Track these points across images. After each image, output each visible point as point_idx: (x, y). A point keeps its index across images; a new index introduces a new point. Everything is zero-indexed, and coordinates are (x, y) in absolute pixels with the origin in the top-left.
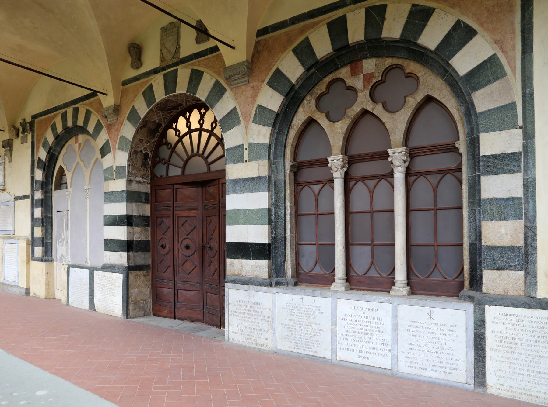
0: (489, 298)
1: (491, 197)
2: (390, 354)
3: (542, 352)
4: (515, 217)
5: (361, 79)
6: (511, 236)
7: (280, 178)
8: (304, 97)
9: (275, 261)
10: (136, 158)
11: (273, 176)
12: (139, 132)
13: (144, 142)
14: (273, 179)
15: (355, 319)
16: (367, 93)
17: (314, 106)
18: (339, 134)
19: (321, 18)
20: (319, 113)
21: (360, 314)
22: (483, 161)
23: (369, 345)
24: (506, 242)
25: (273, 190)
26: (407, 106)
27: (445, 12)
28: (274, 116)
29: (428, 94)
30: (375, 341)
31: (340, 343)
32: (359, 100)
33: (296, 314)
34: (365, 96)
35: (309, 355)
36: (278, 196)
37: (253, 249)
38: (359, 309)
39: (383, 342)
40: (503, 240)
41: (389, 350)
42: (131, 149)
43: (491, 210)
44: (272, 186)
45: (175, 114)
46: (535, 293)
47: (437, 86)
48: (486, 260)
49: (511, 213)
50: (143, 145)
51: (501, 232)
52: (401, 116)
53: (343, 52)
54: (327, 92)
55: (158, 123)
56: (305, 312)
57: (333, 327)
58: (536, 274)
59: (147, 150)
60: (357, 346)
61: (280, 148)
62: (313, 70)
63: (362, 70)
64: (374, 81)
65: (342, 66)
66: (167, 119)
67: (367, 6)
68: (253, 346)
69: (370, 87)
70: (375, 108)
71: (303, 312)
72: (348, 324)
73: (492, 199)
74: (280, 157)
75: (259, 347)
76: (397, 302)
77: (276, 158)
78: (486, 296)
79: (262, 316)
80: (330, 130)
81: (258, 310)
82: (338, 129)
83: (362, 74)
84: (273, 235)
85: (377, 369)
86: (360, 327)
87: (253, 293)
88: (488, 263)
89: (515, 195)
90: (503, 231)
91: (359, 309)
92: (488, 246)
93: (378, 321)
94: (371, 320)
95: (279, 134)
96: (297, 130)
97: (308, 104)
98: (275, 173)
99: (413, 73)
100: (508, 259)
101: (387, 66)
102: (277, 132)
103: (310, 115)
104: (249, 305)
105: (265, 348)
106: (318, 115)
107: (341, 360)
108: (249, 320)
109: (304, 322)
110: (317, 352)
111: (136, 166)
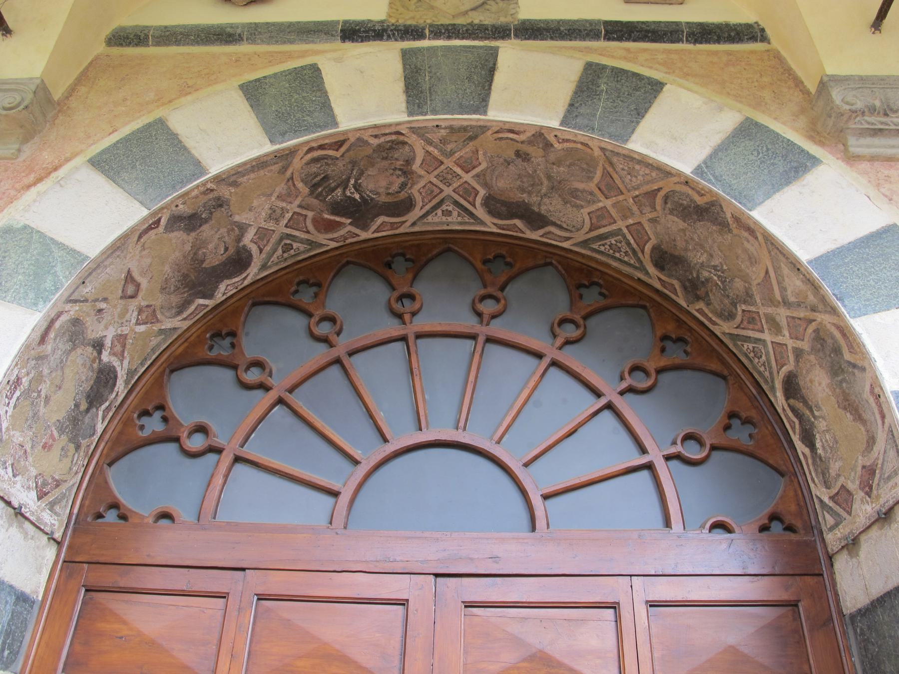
10: (62, 365)
12: (152, 233)
13: (133, 304)
42: (69, 301)
45: (333, 245)
50: (122, 315)
55: (244, 246)
59: (122, 357)
66: (287, 248)
111: (42, 410)
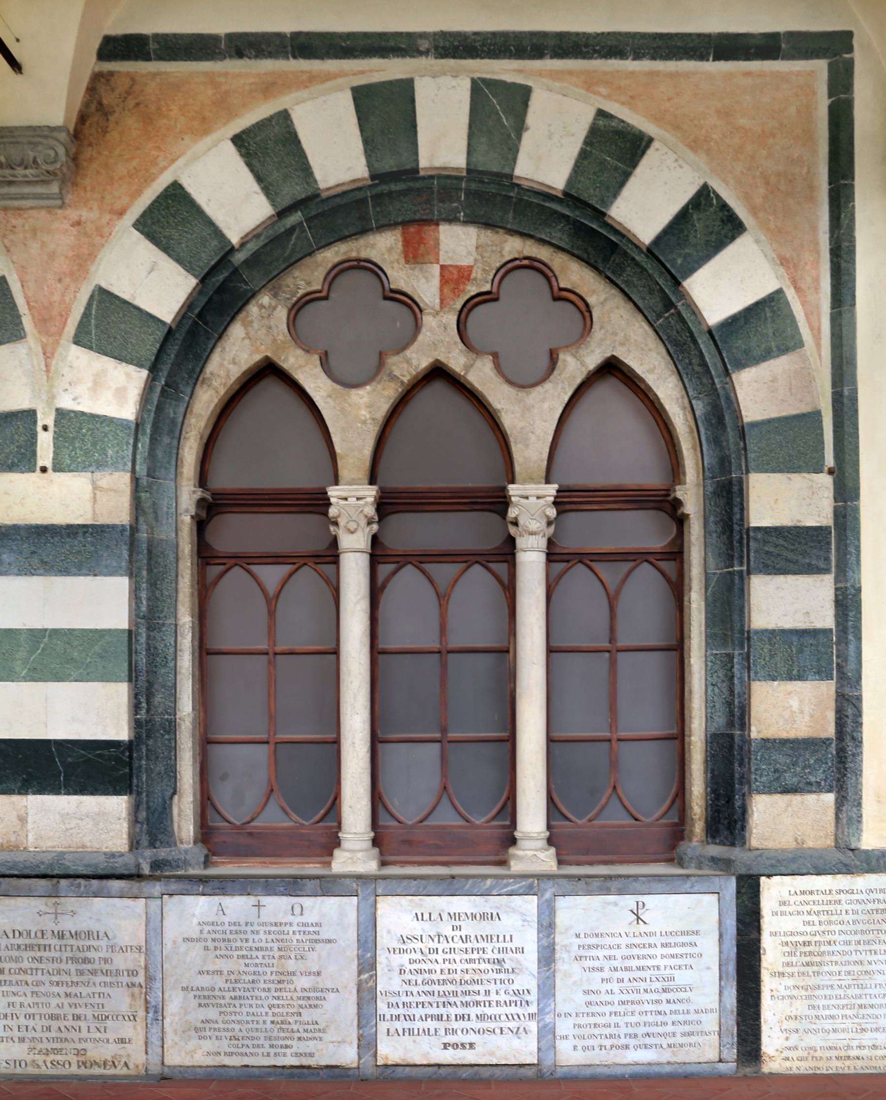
0: (768, 858)
1: (771, 626)
2: (533, 1026)
3: (870, 963)
4: (818, 673)
5: (433, 277)
6: (812, 716)
7: (163, 537)
8: (253, 295)
9: (147, 796)
11: (143, 527)
14: (143, 535)
15: (435, 945)
16: (451, 319)
17: (284, 327)
18: (364, 422)
19: (332, 65)
20: (299, 352)
21: (448, 931)
22: (755, 539)
23: (473, 1011)
24: (801, 729)
25: (144, 573)
26: (560, 374)
27: (675, 156)
28: (160, 334)
29: (614, 354)
30: (493, 997)
31: (388, 1017)
32: (425, 336)
33: (235, 953)
34: (445, 328)
35: (284, 1067)
36: (158, 594)
37: (70, 760)
38: (445, 917)
39: (514, 998)
40: (796, 726)
41: (531, 1016)
43: (772, 656)
44: (143, 558)
46: (859, 840)
47: (636, 337)
48: (759, 772)
49: (811, 665)
51: (791, 706)
52: (543, 400)
53: (395, 187)
54: (324, 294)
56: (269, 945)
57: (365, 976)
58: (861, 798)
60: (439, 1018)
61: (166, 440)
62: (297, 217)
63: (438, 254)
64: (473, 290)
65: (381, 228)
67: (476, 75)
68: (74, 1070)
69: (458, 305)
70: (472, 365)
71: (263, 945)
72: (411, 962)
73: (774, 630)
74: (166, 468)
75: (96, 1071)
76: (553, 890)
77: (154, 471)
78: (761, 856)
79: (106, 973)
80: (335, 408)
81: (91, 955)
82: (359, 408)
83: (438, 263)
84: (142, 715)
85: (497, 1072)
86: (447, 966)
87: (71, 903)
88: (764, 779)
89: (819, 625)
90: (795, 703)
91: (445, 917)
92: (765, 741)
93: (501, 945)
94: (481, 945)
95: (167, 398)
96: (222, 391)
97: (262, 317)
98: (151, 516)
99: (577, 291)
100: (805, 767)
101: (508, 258)
102: (163, 391)
103: (269, 354)
104: (54, 942)
105: (121, 1071)
106: (297, 357)
107: (390, 1063)
108: (56, 989)
109: (265, 973)
110: (311, 1055)
